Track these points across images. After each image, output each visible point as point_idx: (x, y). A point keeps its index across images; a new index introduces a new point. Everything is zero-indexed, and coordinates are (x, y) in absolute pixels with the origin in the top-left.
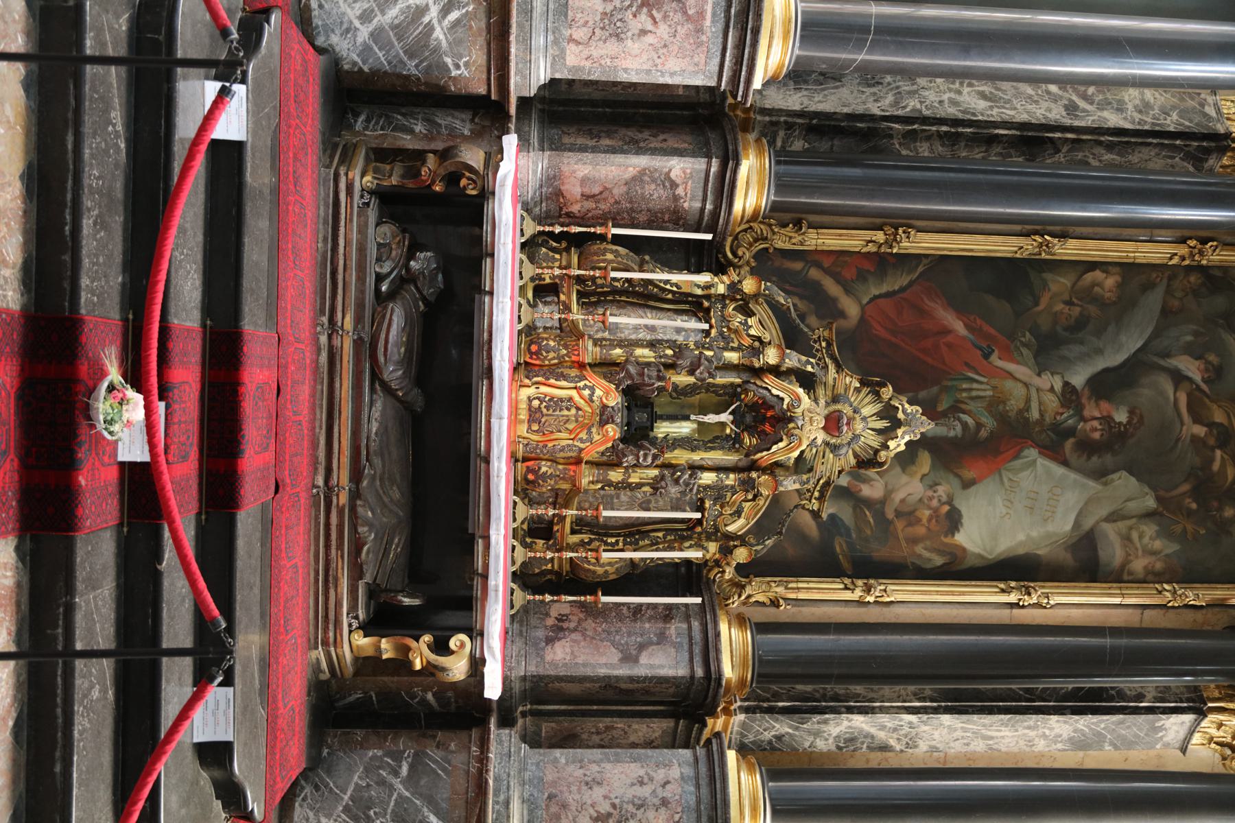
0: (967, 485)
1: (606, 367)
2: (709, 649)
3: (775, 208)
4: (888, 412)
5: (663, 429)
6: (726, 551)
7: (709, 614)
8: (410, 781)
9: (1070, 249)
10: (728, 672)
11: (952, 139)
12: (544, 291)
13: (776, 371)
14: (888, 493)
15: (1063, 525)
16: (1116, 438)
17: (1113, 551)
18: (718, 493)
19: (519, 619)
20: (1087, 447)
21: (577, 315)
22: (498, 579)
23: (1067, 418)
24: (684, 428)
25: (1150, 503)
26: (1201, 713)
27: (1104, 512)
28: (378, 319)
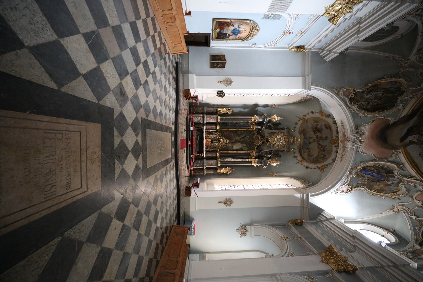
0: (234, 145)
1: (210, 138)
2: (217, 155)
3: (220, 128)
4: (227, 141)
5: (214, 142)
6: (218, 149)
7: (217, 153)
8: (200, 162)
9: (240, 129)
10: (218, 156)
11: (231, 123)
12: (206, 134)
13: (220, 138)
14: (229, 145)
15: (240, 147)
16: (243, 141)
17: (244, 149)
18: (217, 146)
19: (206, 153)
20: (242, 142)
21: (208, 135)
22: (205, 150)
23: (240, 140)
24: (215, 142)
25: (246, 145)
26: (249, 159)
27: (243, 146)
28: (197, 137)
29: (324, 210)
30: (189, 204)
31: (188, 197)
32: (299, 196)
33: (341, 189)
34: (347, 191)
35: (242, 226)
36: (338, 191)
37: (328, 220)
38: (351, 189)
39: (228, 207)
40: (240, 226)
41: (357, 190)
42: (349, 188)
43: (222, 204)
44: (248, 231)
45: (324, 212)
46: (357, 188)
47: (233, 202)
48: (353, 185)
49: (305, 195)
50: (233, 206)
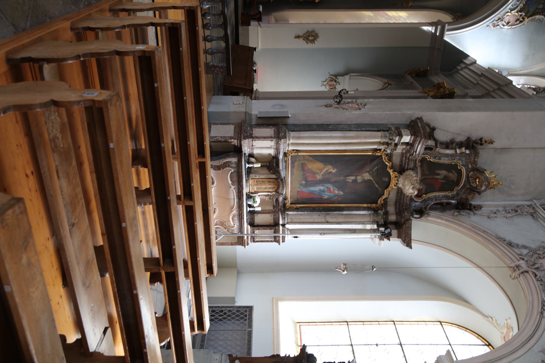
29: (469, 56)
30: (248, 38)
31: (247, 27)
32: (430, 29)
33: (507, 19)
34: (516, 21)
35: (330, 77)
36: (500, 23)
37: (467, 66)
38: (523, 18)
39: (310, 46)
40: (327, 76)
41: (532, 20)
42: (521, 17)
43: (301, 39)
44: (339, 84)
45: (469, 58)
46: (534, 17)
47: (318, 37)
48: (528, 12)
49: (439, 27)
50: (318, 44)
